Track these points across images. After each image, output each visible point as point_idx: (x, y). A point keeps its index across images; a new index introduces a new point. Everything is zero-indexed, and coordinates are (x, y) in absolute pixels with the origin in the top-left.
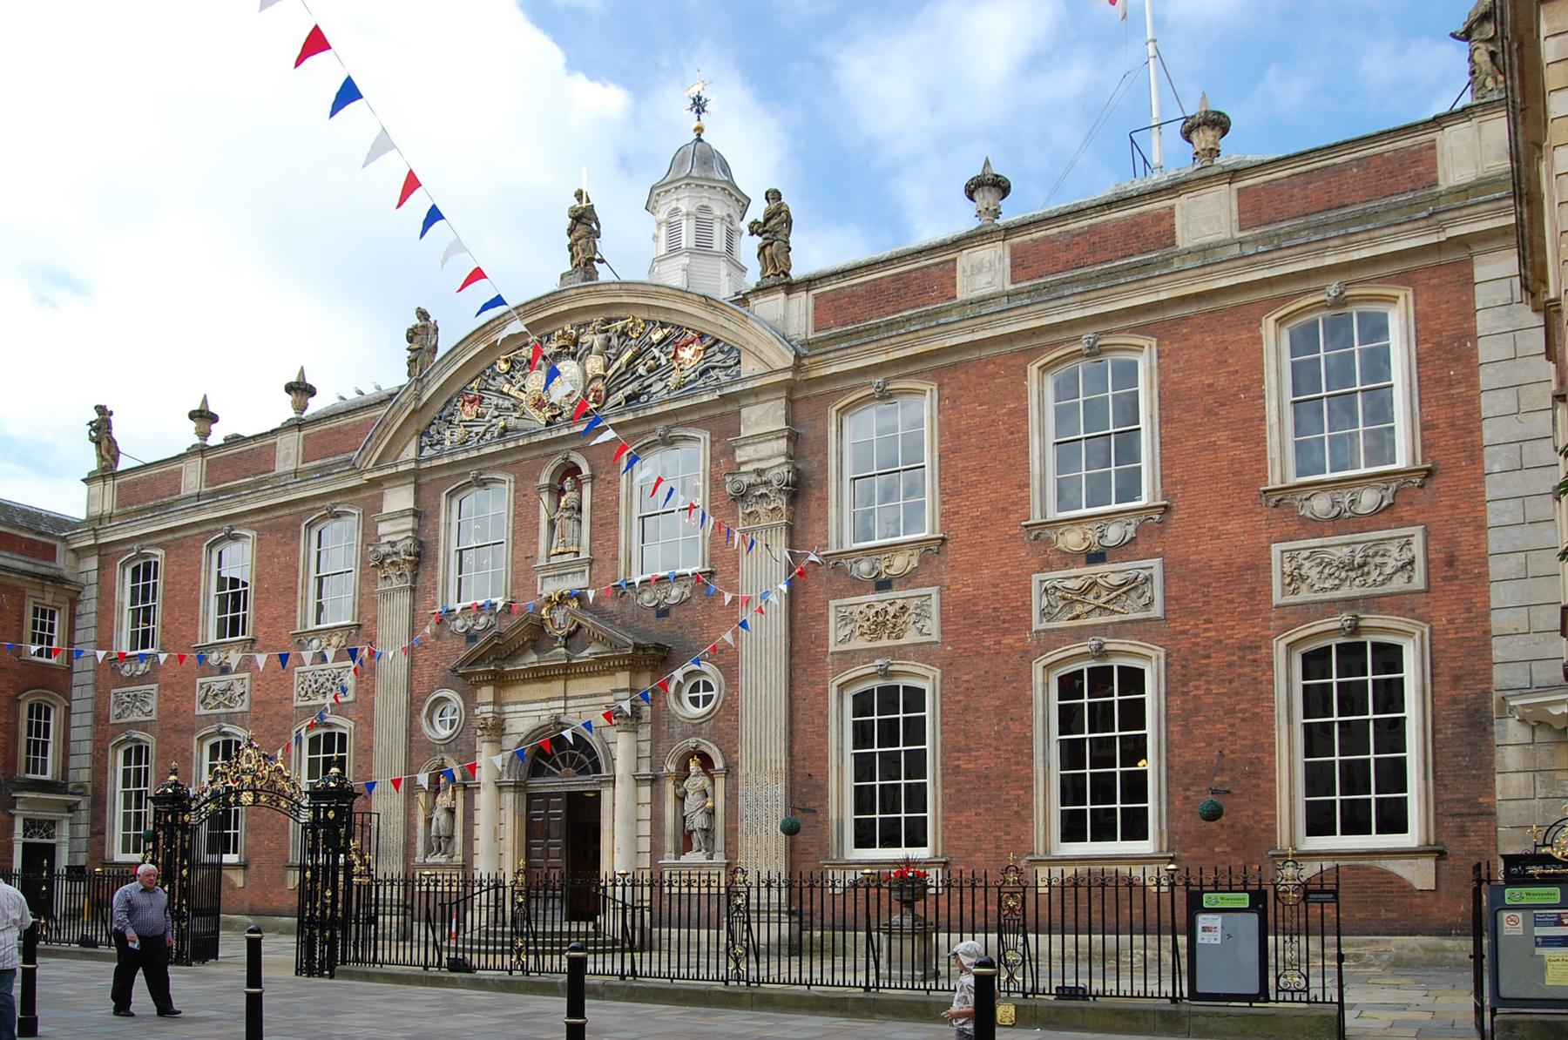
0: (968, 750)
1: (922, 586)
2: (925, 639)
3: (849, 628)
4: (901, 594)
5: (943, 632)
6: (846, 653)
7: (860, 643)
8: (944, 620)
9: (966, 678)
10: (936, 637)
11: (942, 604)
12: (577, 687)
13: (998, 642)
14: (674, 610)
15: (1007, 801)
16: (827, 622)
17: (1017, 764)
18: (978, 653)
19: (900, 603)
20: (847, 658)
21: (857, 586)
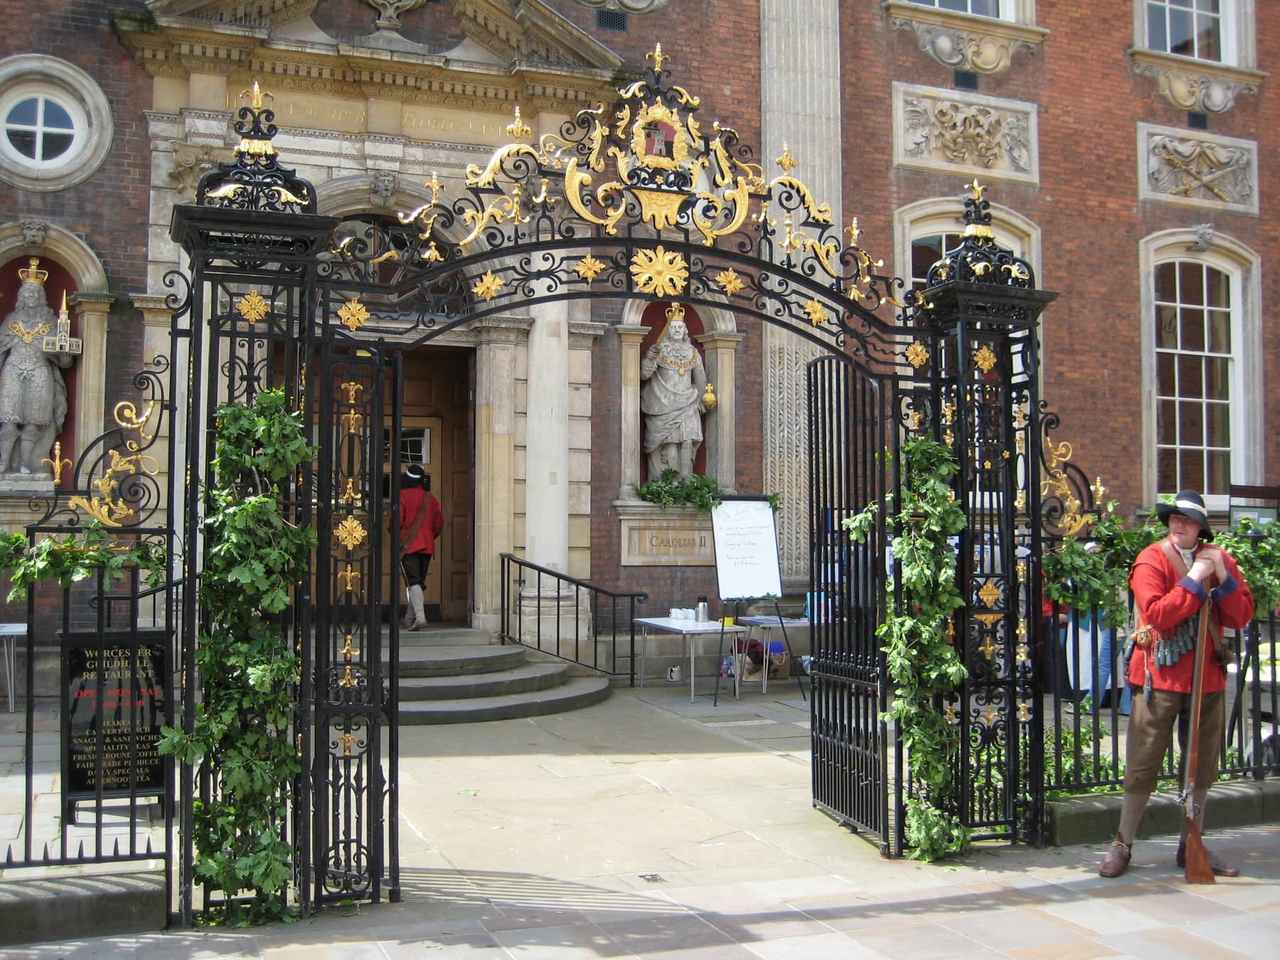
0: (1071, 351)
1: (1013, 96)
2: (1021, 177)
3: (926, 131)
4: (993, 101)
5: (1043, 174)
6: (917, 172)
7: (934, 162)
8: (1043, 157)
9: (1068, 246)
10: (1036, 179)
11: (1042, 132)
12: (424, 119)
13: (1102, 205)
14: (633, 21)
15: (1114, 430)
16: (889, 113)
17: (1125, 379)
18: (1081, 214)
19: (994, 115)
20: (920, 183)
21: (929, 69)
